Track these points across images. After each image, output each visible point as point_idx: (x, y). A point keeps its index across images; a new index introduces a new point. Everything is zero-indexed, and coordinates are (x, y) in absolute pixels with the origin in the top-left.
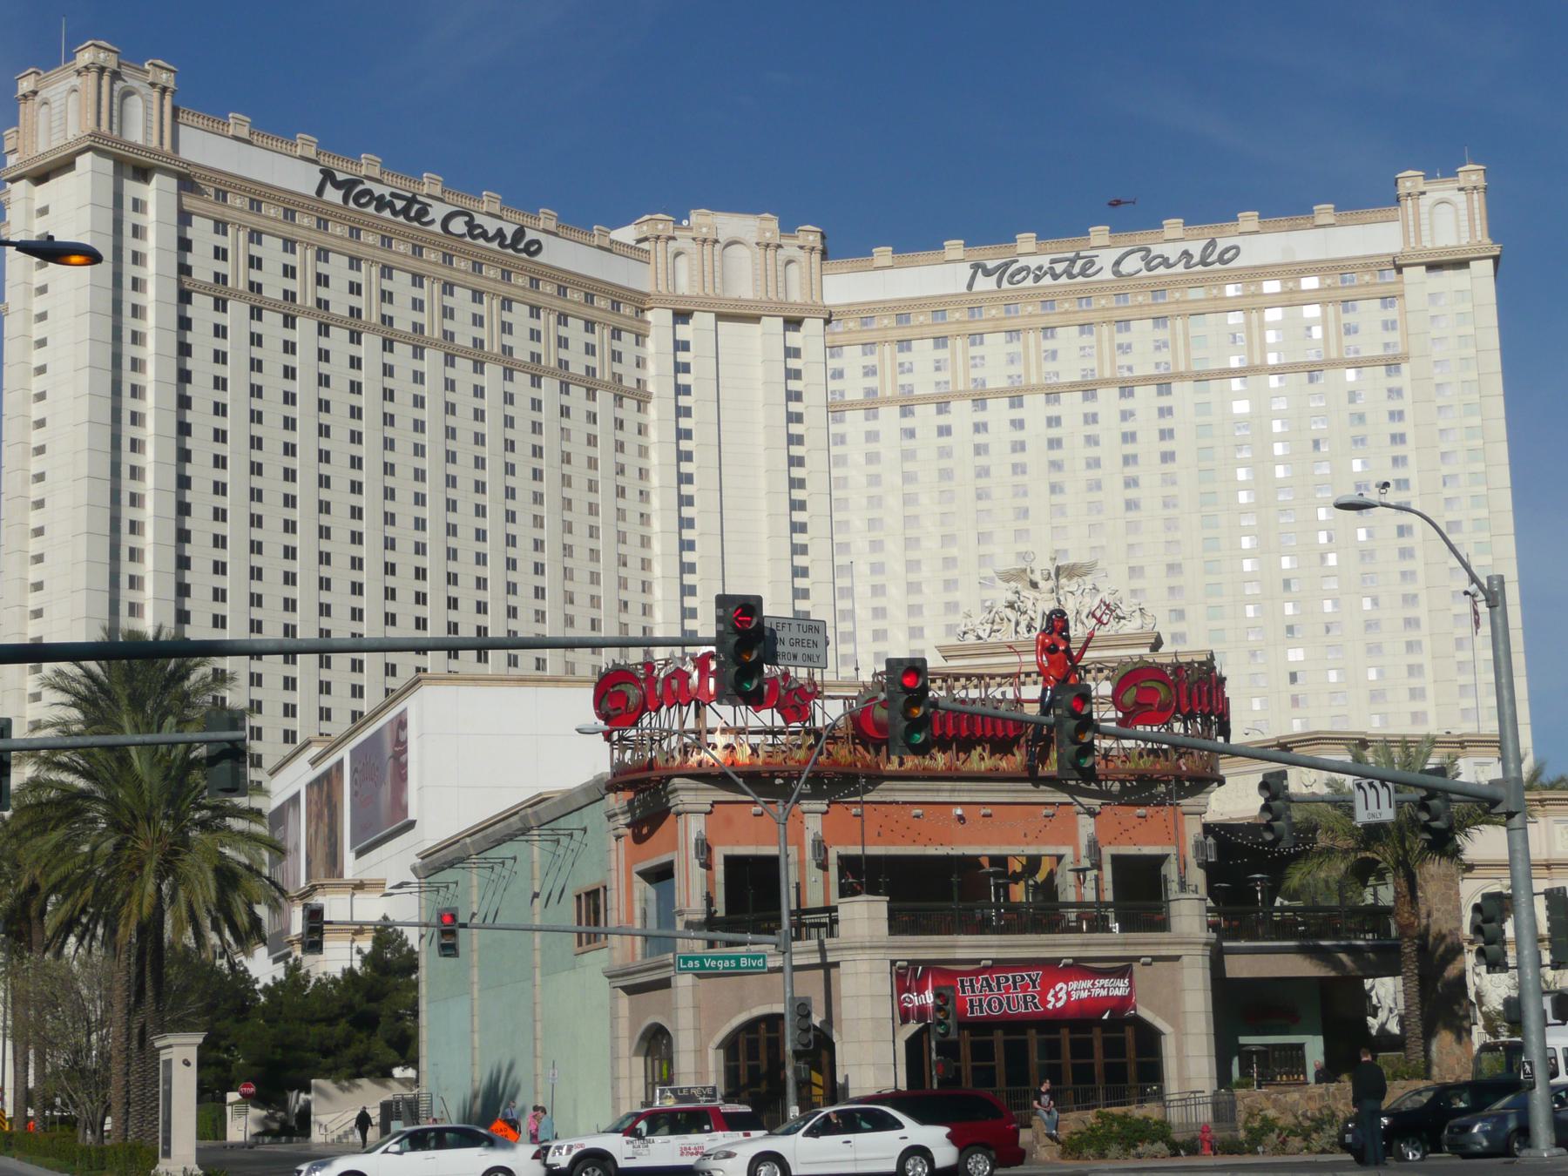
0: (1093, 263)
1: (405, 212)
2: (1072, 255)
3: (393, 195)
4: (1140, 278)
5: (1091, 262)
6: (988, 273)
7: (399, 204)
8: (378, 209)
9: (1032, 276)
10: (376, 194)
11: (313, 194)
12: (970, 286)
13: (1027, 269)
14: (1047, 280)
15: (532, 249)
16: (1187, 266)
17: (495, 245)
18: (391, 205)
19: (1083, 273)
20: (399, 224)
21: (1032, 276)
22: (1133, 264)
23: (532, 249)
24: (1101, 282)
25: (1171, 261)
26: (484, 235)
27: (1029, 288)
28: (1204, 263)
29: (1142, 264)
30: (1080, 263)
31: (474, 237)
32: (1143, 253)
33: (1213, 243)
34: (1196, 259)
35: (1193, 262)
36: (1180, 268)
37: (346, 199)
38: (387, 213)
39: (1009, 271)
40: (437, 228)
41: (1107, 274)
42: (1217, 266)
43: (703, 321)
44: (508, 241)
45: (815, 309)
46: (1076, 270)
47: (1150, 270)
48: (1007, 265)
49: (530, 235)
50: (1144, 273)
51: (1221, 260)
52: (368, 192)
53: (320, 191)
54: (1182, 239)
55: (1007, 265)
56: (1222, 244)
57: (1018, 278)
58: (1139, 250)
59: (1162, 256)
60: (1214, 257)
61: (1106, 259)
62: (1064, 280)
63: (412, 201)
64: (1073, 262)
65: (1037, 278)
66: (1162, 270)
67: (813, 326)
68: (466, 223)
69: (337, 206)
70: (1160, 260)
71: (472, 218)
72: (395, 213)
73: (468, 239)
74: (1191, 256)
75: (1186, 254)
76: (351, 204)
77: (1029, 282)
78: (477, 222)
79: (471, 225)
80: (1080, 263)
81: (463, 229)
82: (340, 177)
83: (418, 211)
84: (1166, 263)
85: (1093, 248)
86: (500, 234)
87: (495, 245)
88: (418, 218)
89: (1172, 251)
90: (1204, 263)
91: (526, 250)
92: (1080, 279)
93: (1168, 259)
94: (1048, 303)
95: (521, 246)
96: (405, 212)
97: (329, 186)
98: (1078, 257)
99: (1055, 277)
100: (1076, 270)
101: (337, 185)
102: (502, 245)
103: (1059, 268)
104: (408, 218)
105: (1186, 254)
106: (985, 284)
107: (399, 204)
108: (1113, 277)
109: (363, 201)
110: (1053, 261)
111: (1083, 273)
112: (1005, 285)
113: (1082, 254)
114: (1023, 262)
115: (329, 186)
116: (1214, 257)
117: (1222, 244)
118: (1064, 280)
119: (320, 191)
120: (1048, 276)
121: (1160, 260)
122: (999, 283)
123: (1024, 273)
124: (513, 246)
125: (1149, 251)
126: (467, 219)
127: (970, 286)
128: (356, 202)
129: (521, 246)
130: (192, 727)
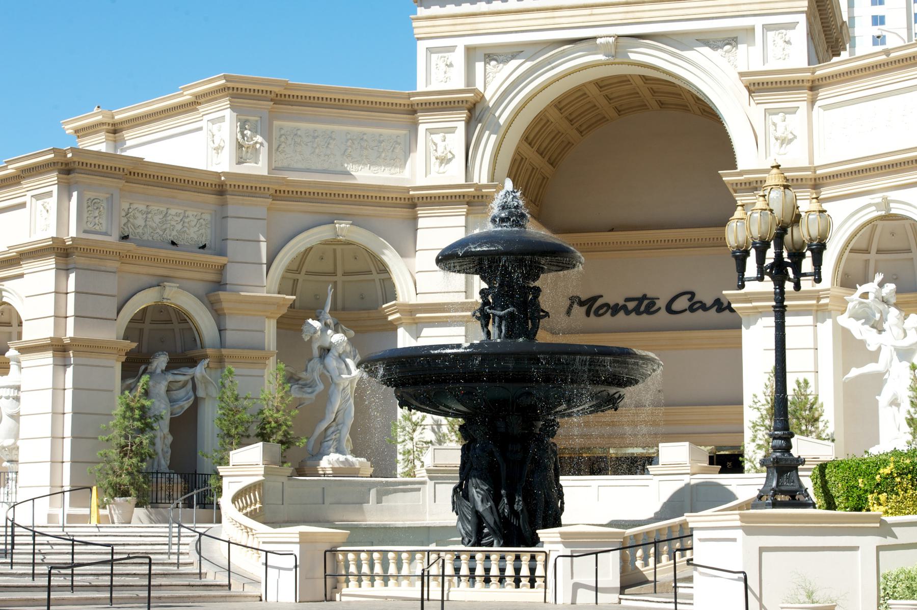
0: (654, 304)
9: (610, 311)
13: (607, 305)
14: (621, 314)
21: (610, 311)
30: (646, 302)
32: (689, 296)
39: (593, 310)
46: (642, 308)
57: (601, 312)
59: (701, 302)
65: (613, 315)
66: (700, 312)
70: (698, 305)
74: (722, 304)
80: (646, 302)
84: (704, 307)
92: (645, 316)
93: (705, 304)
100: (642, 308)
103: (631, 305)
110: (627, 300)
121: (698, 305)
123: (605, 309)
125: (693, 294)
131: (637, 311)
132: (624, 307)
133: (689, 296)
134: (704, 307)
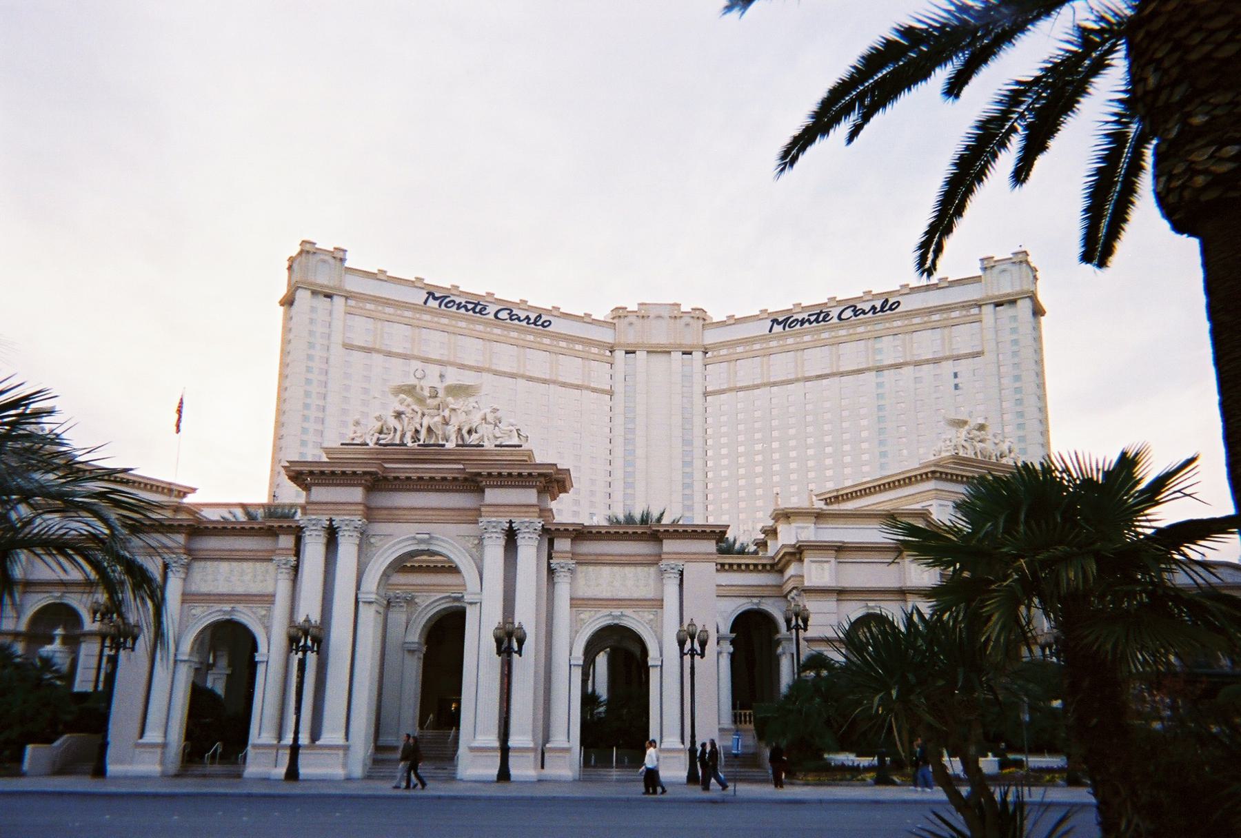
0: (829, 315)
1: (473, 309)
3: (466, 302)
5: (828, 315)
6: (779, 323)
7: (470, 306)
8: (458, 309)
10: (457, 302)
11: (421, 302)
12: (770, 331)
13: (797, 320)
14: (807, 325)
15: (545, 324)
16: (874, 313)
17: (524, 323)
18: (465, 307)
19: (824, 320)
20: (469, 315)
23: (545, 324)
24: (832, 324)
26: (519, 319)
28: (882, 310)
29: (852, 314)
30: (822, 315)
31: (512, 320)
32: (852, 308)
33: (887, 301)
34: (878, 309)
36: (870, 314)
37: (440, 306)
38: (463, 310)
40: (491, 316)
41: (835, 320)
42: (889, 312)
43: (641, 355)
44: (532, 321)
45: (696, 347)
46: (821, 319)
47: (856, 316)
48: (788, 318)
49: (544, 318)
50: (854, 318)
51: (891, 309)
52: (454, 301)
53: (425, 303)
54: (872, 300)
55: (788, 319)
56: (891, 301)
58: (851, 306)
60: (887, 308)
61: (834, 313)
62: (814, 324)
63: (476, 305)
64: (819, 315)
65: (801, 325)
66: (862, 316)
67: (698, 355)
68: (509, 314)
69: (436, 309)
71: (512, 311)
72: (467, 310)
73: (509, 321)
74: (876, 308)
75: (874, 308)
76: (443, 307)
77: (798, 326)
78: (514, 313)
79: (511, 315)
80: (822, 315)
81: (508, 317)
82: (437, 295)
83: (481, 309)
84: (864, 312)
86: (528, 318)
87: (524, 323)
88: (480, 312)
89: (867, 307)
90: (882, 310)
91: (542, 325)
92: (823, 323)
95: (539, 323)
96: (473, 309)
97: (431, 298)
98: (821, 312)
99: (811, 323)
100: (821, 319)
101: (435, 299)
102: (528, 323)
103: (812, 318)
104: (475, 312)
105: (874, 308)
106: (778, 329)
107: (470, 306)
109: (449, 305)
110: (809, 315)
111: (824, 320)
112: (787, 329)
115: (431, 298)
116: (887, 308)
117: (890, 303)
118: (814, 324)
119: (425, 303)
122: (784, 329)
124: (535, 323)
125: (855, 307)
126: (509, 312)
127: (770, 331)
128: (446, 306)
129: (539, 323)
130: (782, 604)
131: (817, 321)
132: (808, 320)
133: (852, 308)
134: (864, 312)
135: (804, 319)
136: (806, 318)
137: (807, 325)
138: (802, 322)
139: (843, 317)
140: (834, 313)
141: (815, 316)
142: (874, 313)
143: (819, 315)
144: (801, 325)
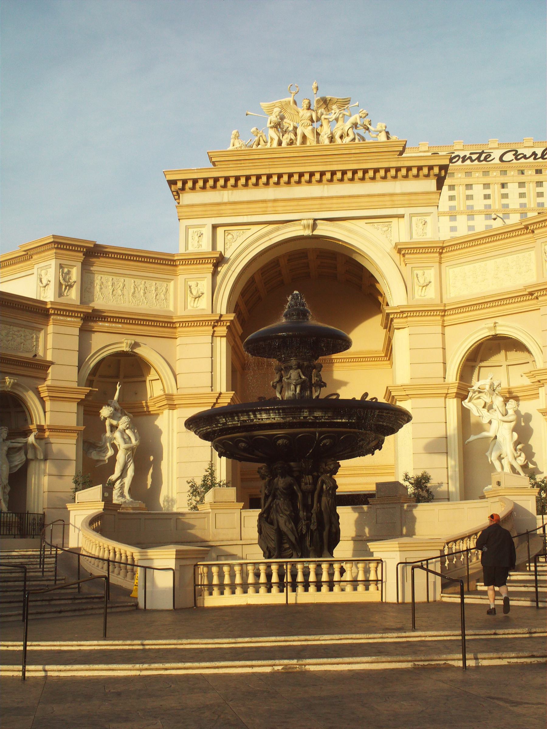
0: (490, 156)
2: (481, 151)
4: (512, 163)
9: (461, 160)
14: (468, 162)
16: (535, 159)
22: (509, 157)
25: (527, 156)
27: (460, 166)
29: (513, 157)
30: (483, 156)
32: (514, 152)
34: (539, 156)
35: (537, 157)
36: (531, 159)
41: (497, 161)
46: (482, 158)
50: (515, 161)
54: (532, 147)
57: (454, 161)
59: (523, 154)
61: (496, 154)
64: (481, 154)
65: (463, 162)
66: (523, 160)
74: (536, 155)
75: (534, 154)
77: (460, 162)
80: (483, 156)
84: (525, 157)
85: (490, 149)
92: (484, 162)
93: (526, 155)
94: (468, 174)
99: (472, 161)
100: (482, 158)
103: (474, 157)
105: (534, 154)
108: (500, 162)
110: (471, 154)
111: (485, 159)
113: (485, 151)
114: (456, 153)
118: (476, 162)
120: (469, 160)
121: (522, 156)
123: (457, 158)
125: (517, 151)
131: (478, 159)
133: (514, 152)
134: (525, 157)
135: (465, 156)
136: (468, 156)
137: (468, 162)
138: (464, 159)
139: (506, 158)
140: (496, 154)
141: (478, 155)
142: (535, 159)
143: (481, 154)
144: (463, 162)
